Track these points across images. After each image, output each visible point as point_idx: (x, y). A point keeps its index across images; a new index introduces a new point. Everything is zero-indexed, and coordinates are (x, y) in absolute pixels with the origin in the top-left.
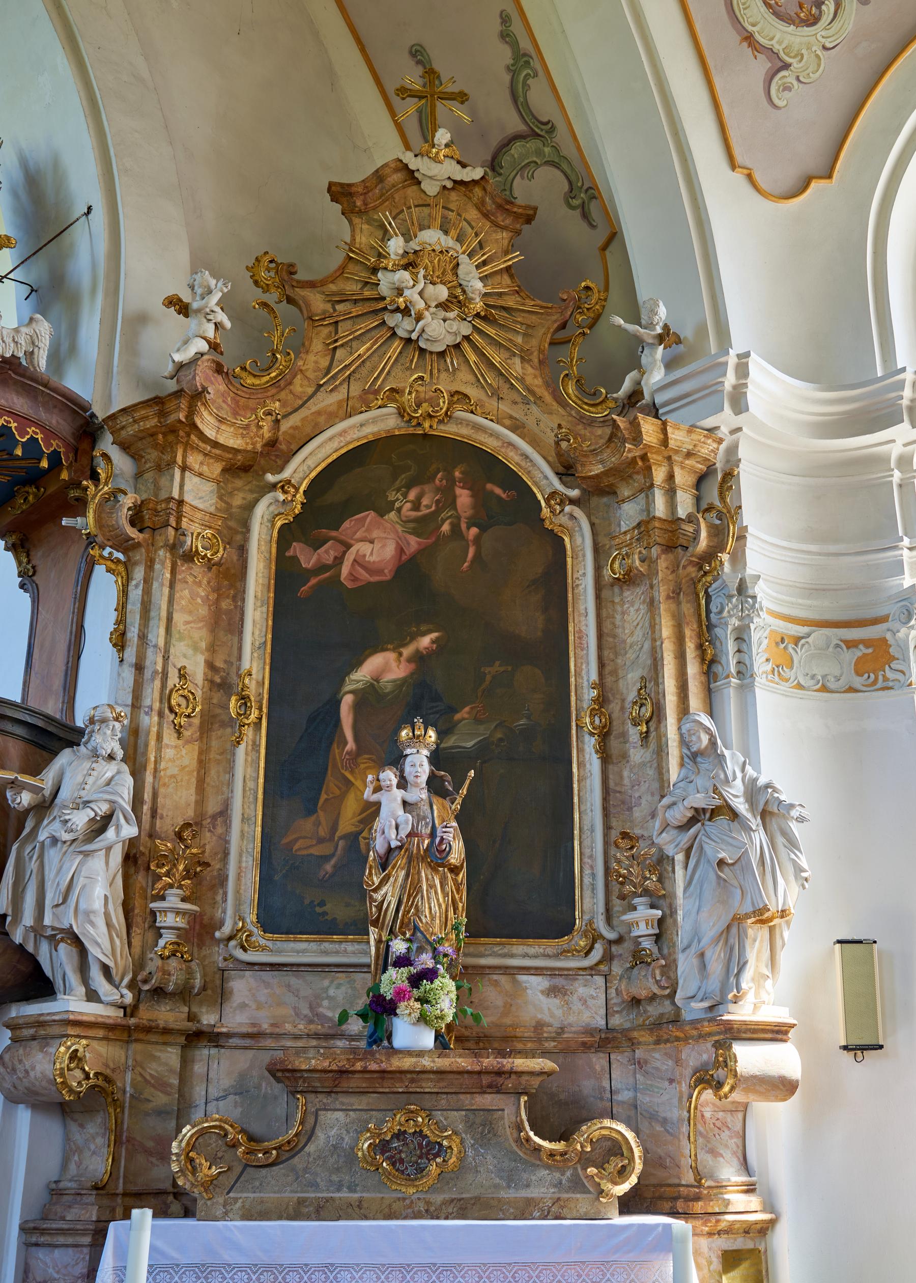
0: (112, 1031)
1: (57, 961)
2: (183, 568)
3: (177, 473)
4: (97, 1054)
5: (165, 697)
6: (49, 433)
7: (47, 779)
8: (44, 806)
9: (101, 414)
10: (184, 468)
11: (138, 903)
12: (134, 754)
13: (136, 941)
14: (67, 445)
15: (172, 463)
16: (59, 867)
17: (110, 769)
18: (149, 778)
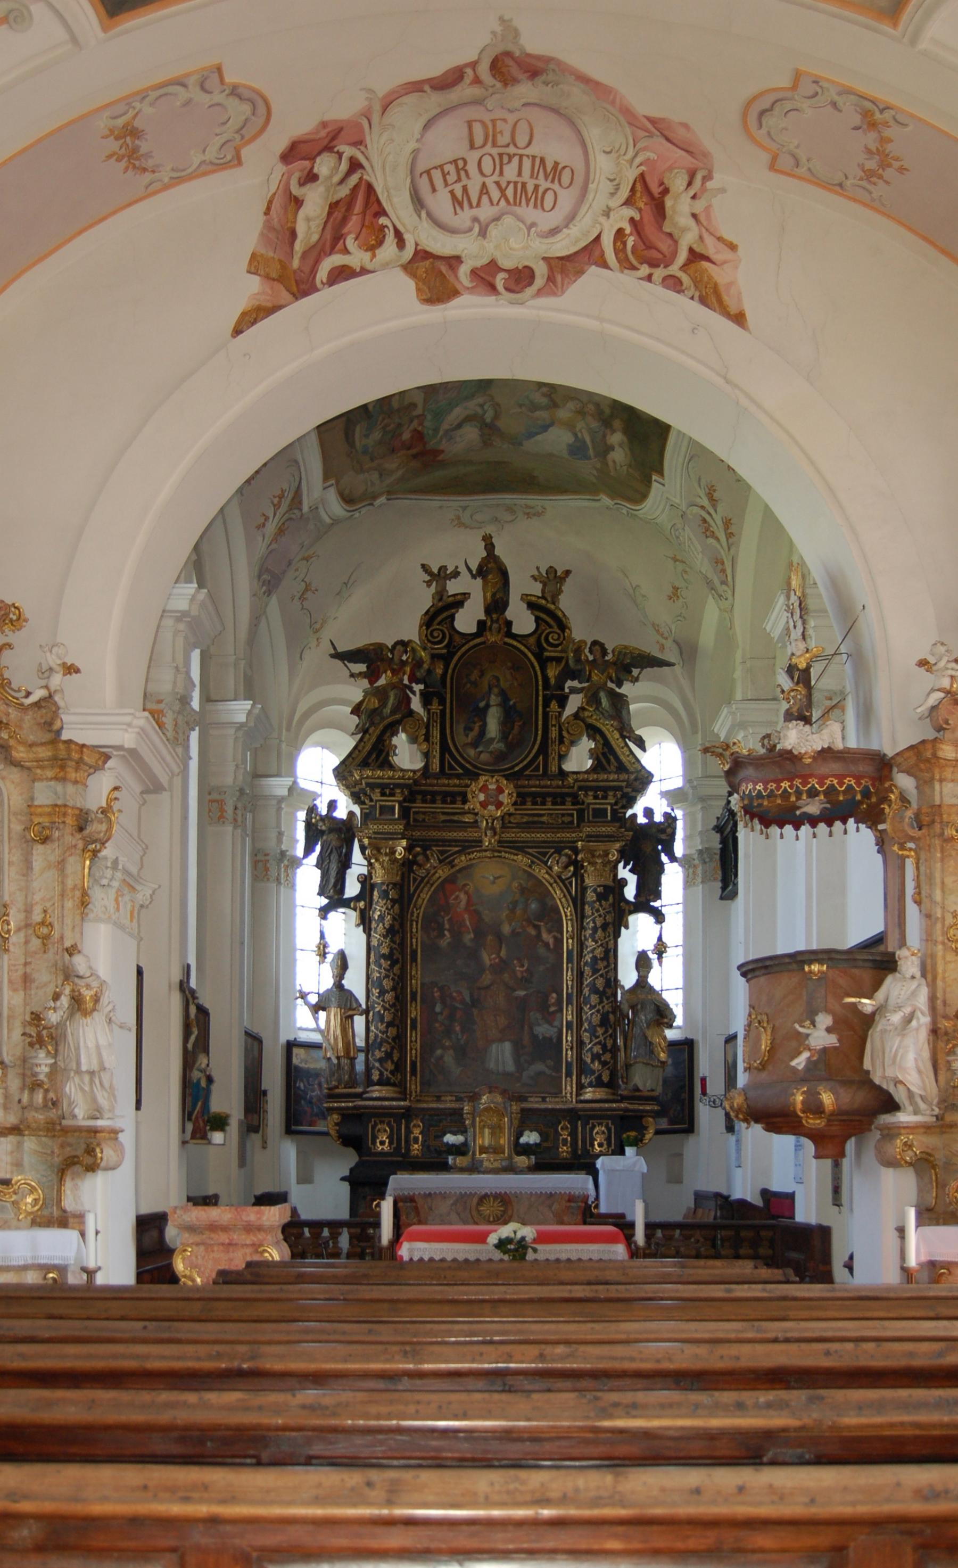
0: (927, 1128)
1: (900, 1095)
2: (948, 846)
3: (937, 786)
4: (920, 1143)
5: (945, 933)
6: (858, 779)
7: (880, 995)
8: (880, 1010)
9: (890, 752)
10: (941, 781)
11: (940, 1056)
12: (927, 971)
13: (942, 1078)
14: (873, 779)
15: (932, 779)
16: (894, 1043)
17: (914, 984)
18: (939, 983)
